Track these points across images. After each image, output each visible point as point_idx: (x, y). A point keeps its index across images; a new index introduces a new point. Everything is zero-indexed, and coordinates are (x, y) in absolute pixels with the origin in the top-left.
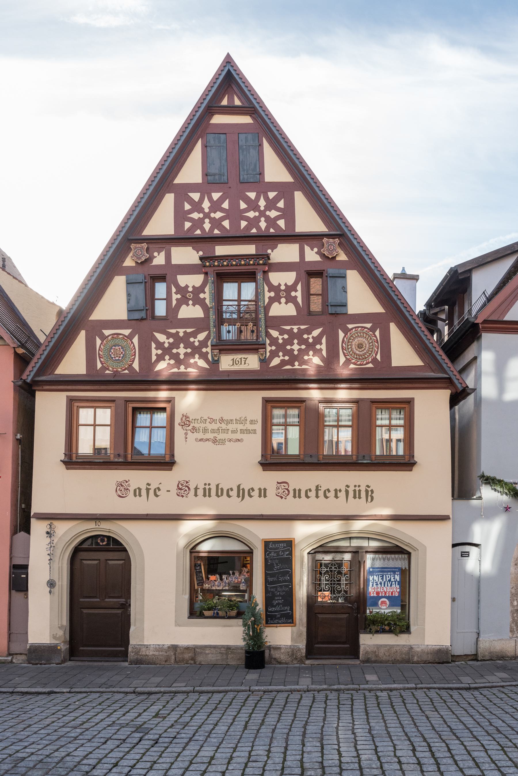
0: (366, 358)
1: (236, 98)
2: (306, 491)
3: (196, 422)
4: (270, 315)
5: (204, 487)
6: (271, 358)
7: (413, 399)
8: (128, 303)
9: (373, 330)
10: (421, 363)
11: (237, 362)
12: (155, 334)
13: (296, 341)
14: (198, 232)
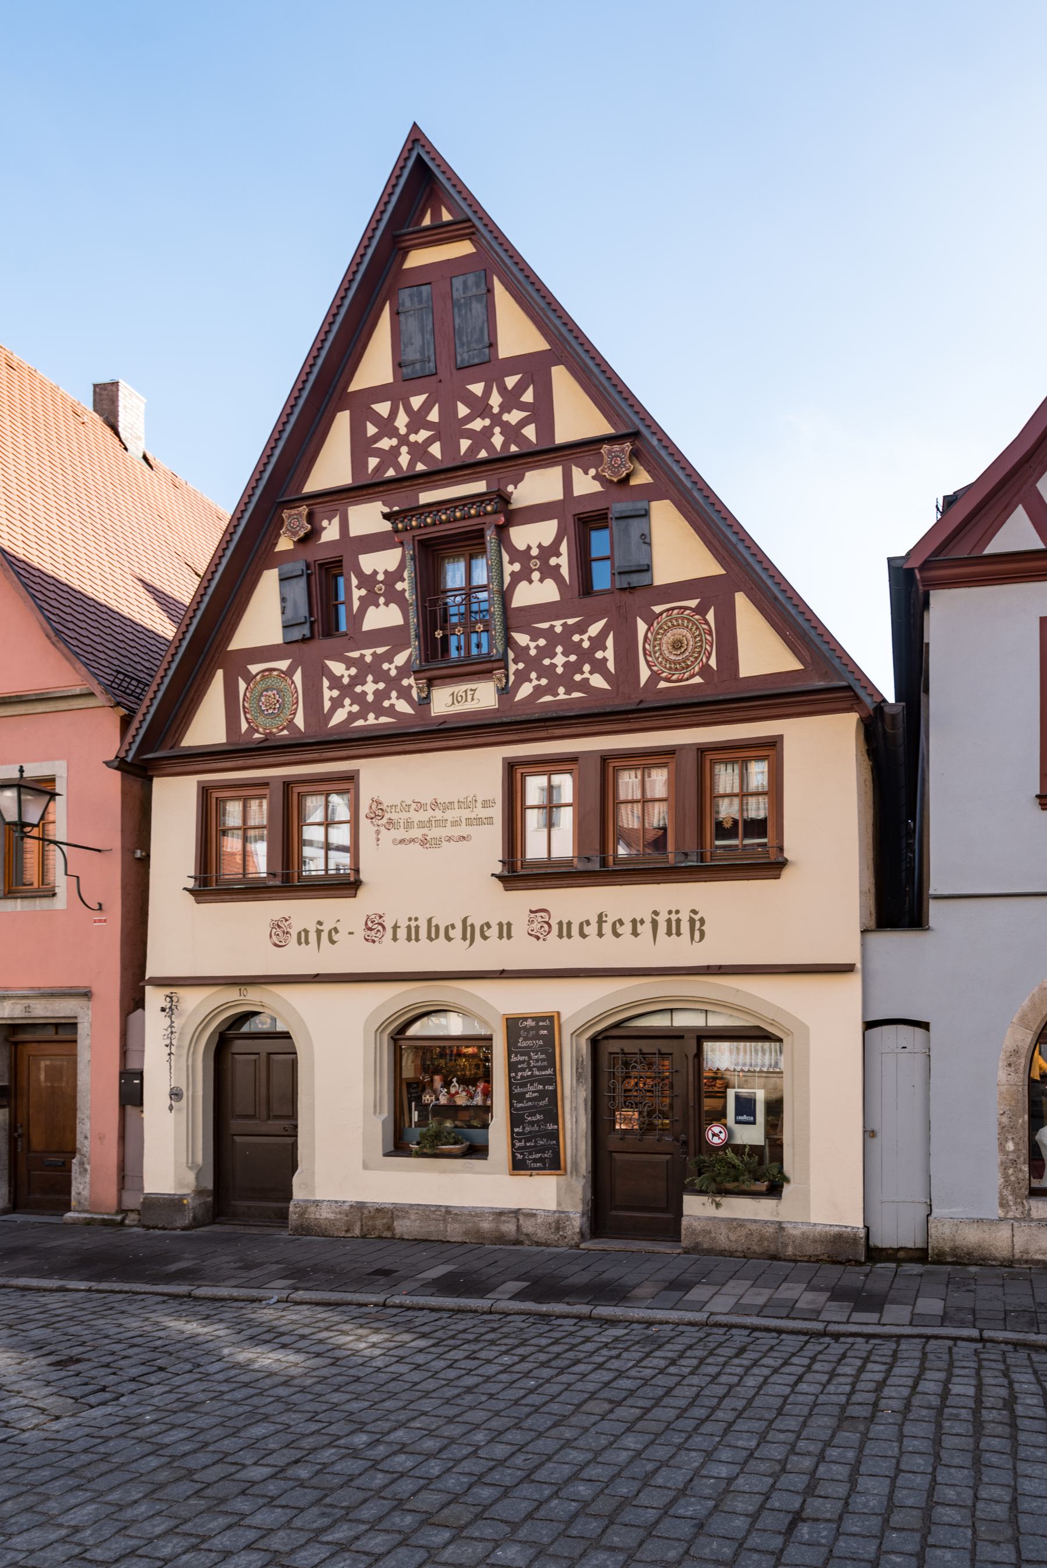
0: (688, 666)
2: (581, 925)
5: (408, 923)
6: (518, 684)
7: (781, 737)
8: (283, 613)
9: (701, 610)
10: (797, 666)
11: (459, 699)
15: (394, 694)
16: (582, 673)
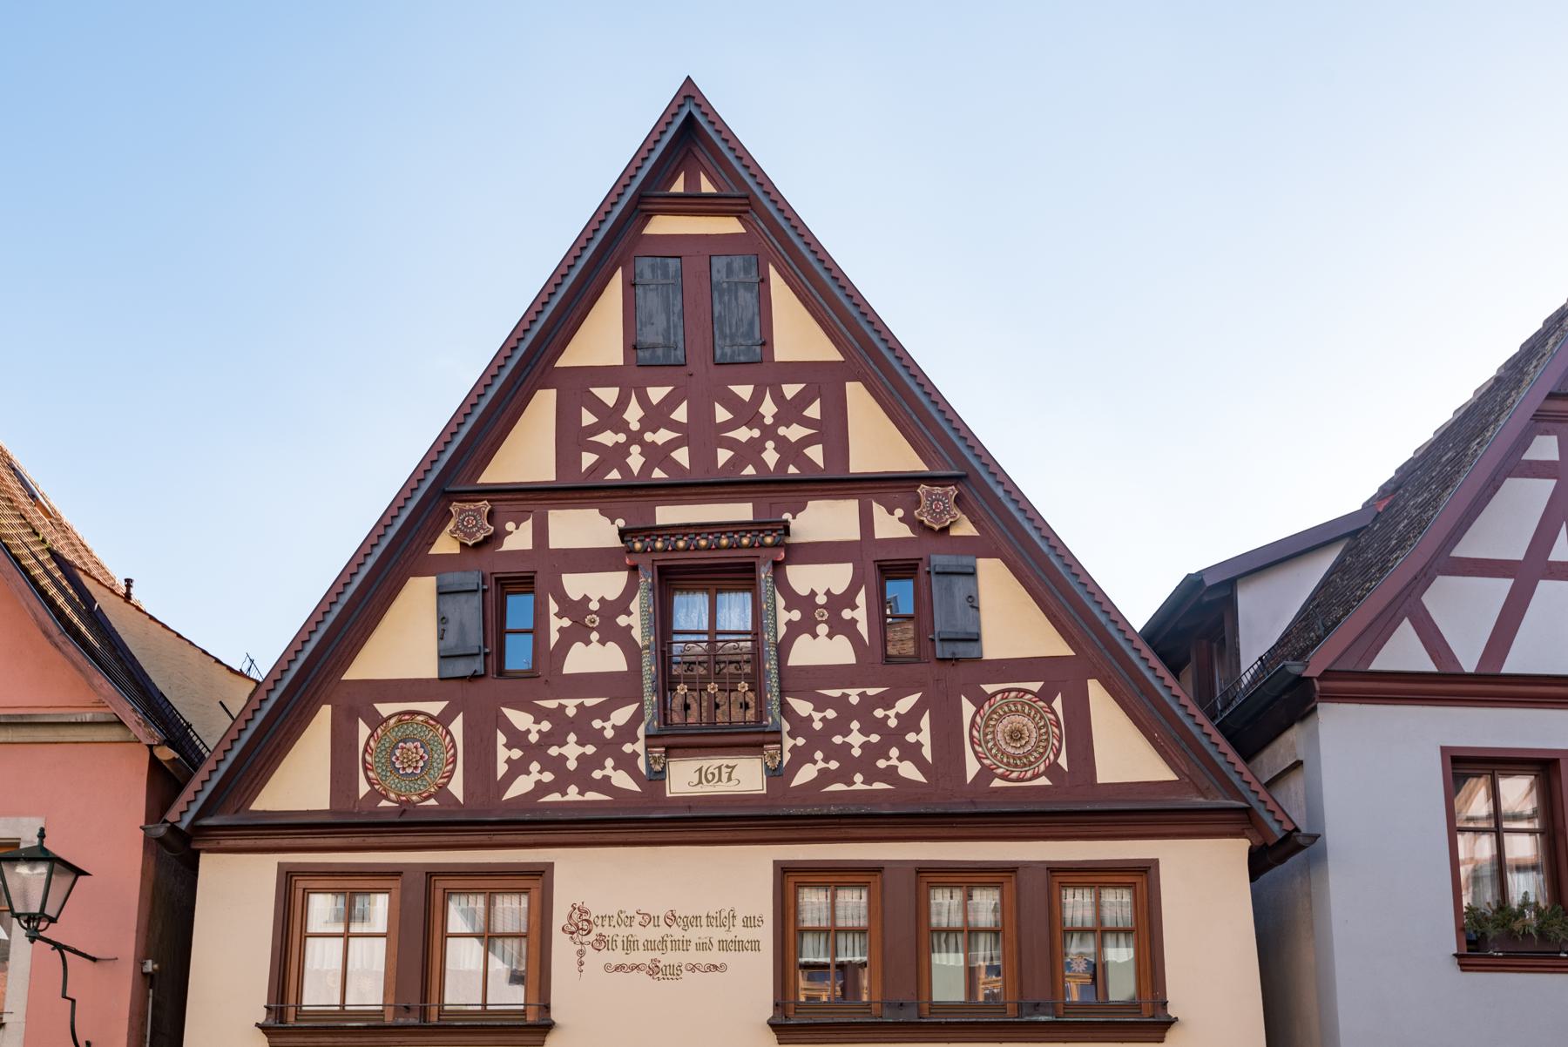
0: (1031, 763)
1: (703, 178)
3: (606, 923)
4: (790, 663)
7: (1156, 862)
8: (441, 638)
9: (1046, 696)
10: (1170, 776)
12: (506, 711)
13: (855, 725)
14: (615, 475)
15: (609, 762)
16: (888, 758)
